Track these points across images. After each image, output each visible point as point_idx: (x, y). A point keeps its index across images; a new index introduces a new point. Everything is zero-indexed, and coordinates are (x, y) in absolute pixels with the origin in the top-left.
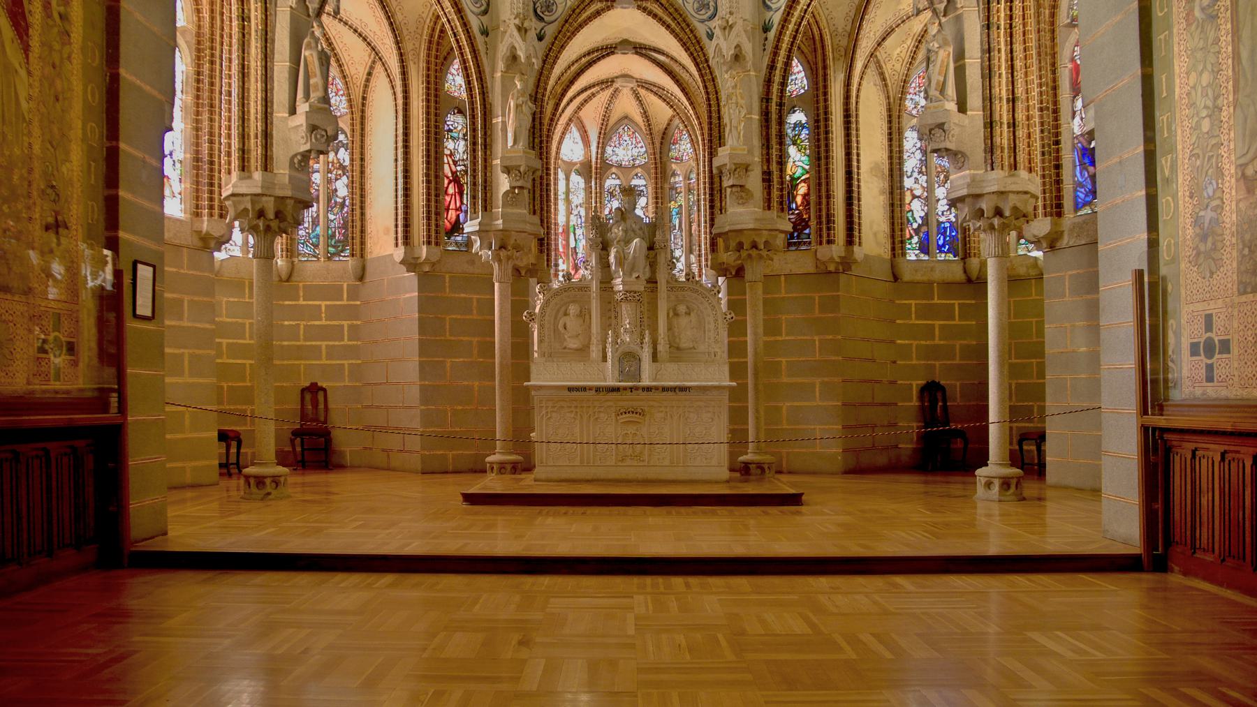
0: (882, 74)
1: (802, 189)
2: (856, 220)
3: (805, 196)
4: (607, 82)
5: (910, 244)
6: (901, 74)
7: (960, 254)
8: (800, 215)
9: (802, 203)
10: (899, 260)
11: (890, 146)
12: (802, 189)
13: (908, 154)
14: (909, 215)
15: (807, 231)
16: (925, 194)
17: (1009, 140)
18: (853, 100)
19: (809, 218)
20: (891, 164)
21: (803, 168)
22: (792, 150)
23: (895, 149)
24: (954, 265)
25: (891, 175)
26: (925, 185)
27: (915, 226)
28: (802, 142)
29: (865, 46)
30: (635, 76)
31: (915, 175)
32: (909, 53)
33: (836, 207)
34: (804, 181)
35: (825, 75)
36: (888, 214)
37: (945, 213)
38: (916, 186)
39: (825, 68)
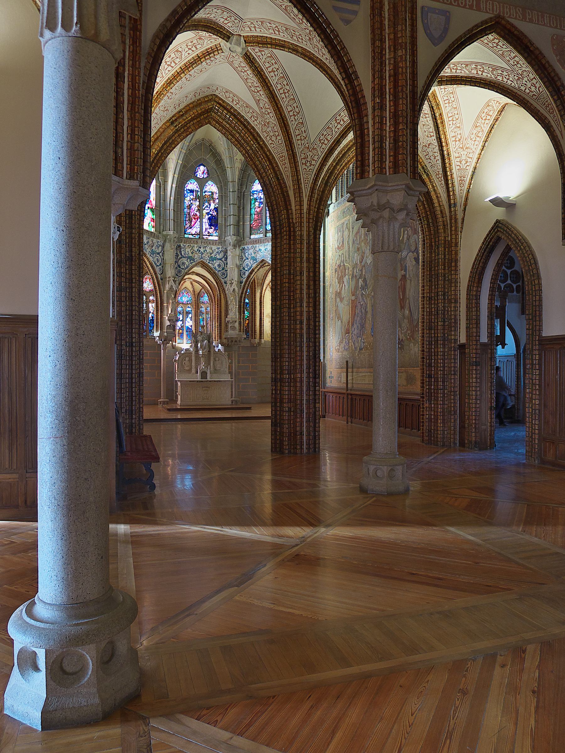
18: (262, 298)
39: (255, 288)
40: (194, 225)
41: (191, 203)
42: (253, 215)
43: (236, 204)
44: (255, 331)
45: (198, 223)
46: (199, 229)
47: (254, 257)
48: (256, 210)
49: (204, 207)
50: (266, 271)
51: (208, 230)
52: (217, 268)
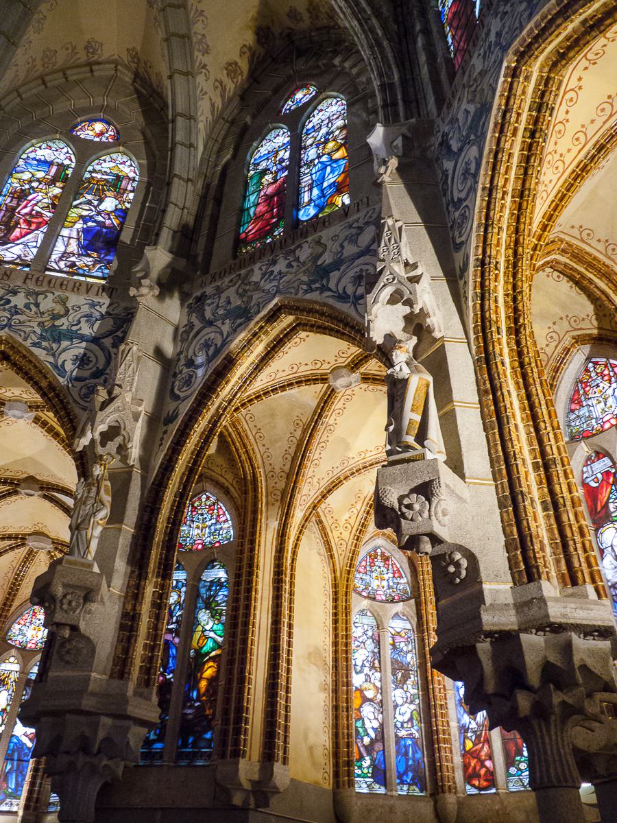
0: (323, 530)
1: (209, 672)
2: (281, 721)
3: (212, 681)
4: (16, 538)
5: (360, 767)
6: (350, 543)
7: (428, 787)
8: (201, 709)
9: (207, 690)
10: (345, 792)
11: (335, 629)
12: (209, 672)
13: (357, 643)
14: (359, 724)
15: (208, 736)
16: (379, 697)
17: (550, 530)
18: (288, 555)
19: (214, 714)
20: (336, 652)
21: (215, 641)
22: (203, 616)
23: (341, 633)
24: (421, 804)
25: (336, 667)
26: (378, 684)
27: (367, 741)
28: (218, 605)
29: (307, 492)
30: (50, 534)
31: (366, 670)
32: (359, 519)
33: (252, 697)
34: (213, 659)
35: (255, 520)
36: (330, 721)
37: (405, 725)
38: (367, 685)
39: (255, 511)
40: (18, 239)
41: (32, 188)
42: (252, 211)
43: (189, 180)
44: (240, 710)
45: (40, 235)
46: (35, 251)
47: (238, 307)
48: (262, 193)
49: (75, 203)
50: (304, 431)
51: (73, 259)
52: (69, 366)
